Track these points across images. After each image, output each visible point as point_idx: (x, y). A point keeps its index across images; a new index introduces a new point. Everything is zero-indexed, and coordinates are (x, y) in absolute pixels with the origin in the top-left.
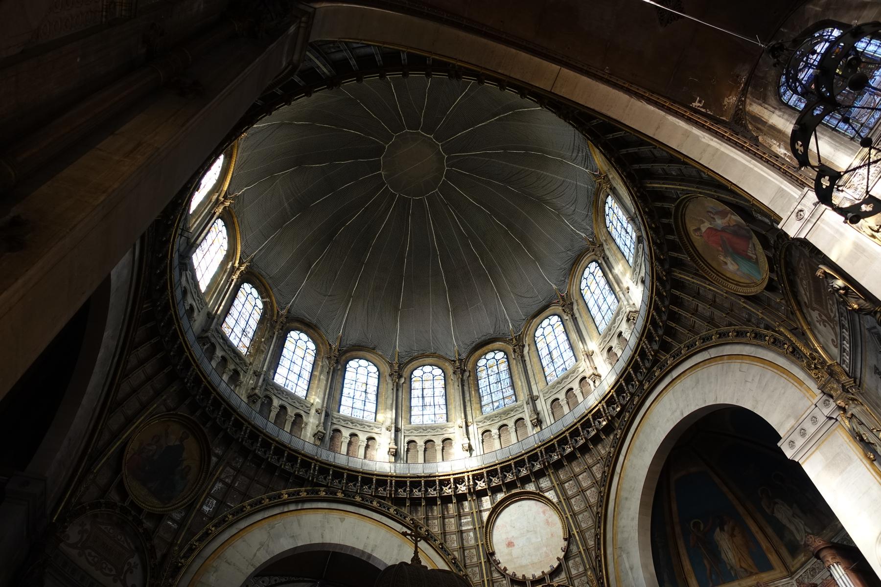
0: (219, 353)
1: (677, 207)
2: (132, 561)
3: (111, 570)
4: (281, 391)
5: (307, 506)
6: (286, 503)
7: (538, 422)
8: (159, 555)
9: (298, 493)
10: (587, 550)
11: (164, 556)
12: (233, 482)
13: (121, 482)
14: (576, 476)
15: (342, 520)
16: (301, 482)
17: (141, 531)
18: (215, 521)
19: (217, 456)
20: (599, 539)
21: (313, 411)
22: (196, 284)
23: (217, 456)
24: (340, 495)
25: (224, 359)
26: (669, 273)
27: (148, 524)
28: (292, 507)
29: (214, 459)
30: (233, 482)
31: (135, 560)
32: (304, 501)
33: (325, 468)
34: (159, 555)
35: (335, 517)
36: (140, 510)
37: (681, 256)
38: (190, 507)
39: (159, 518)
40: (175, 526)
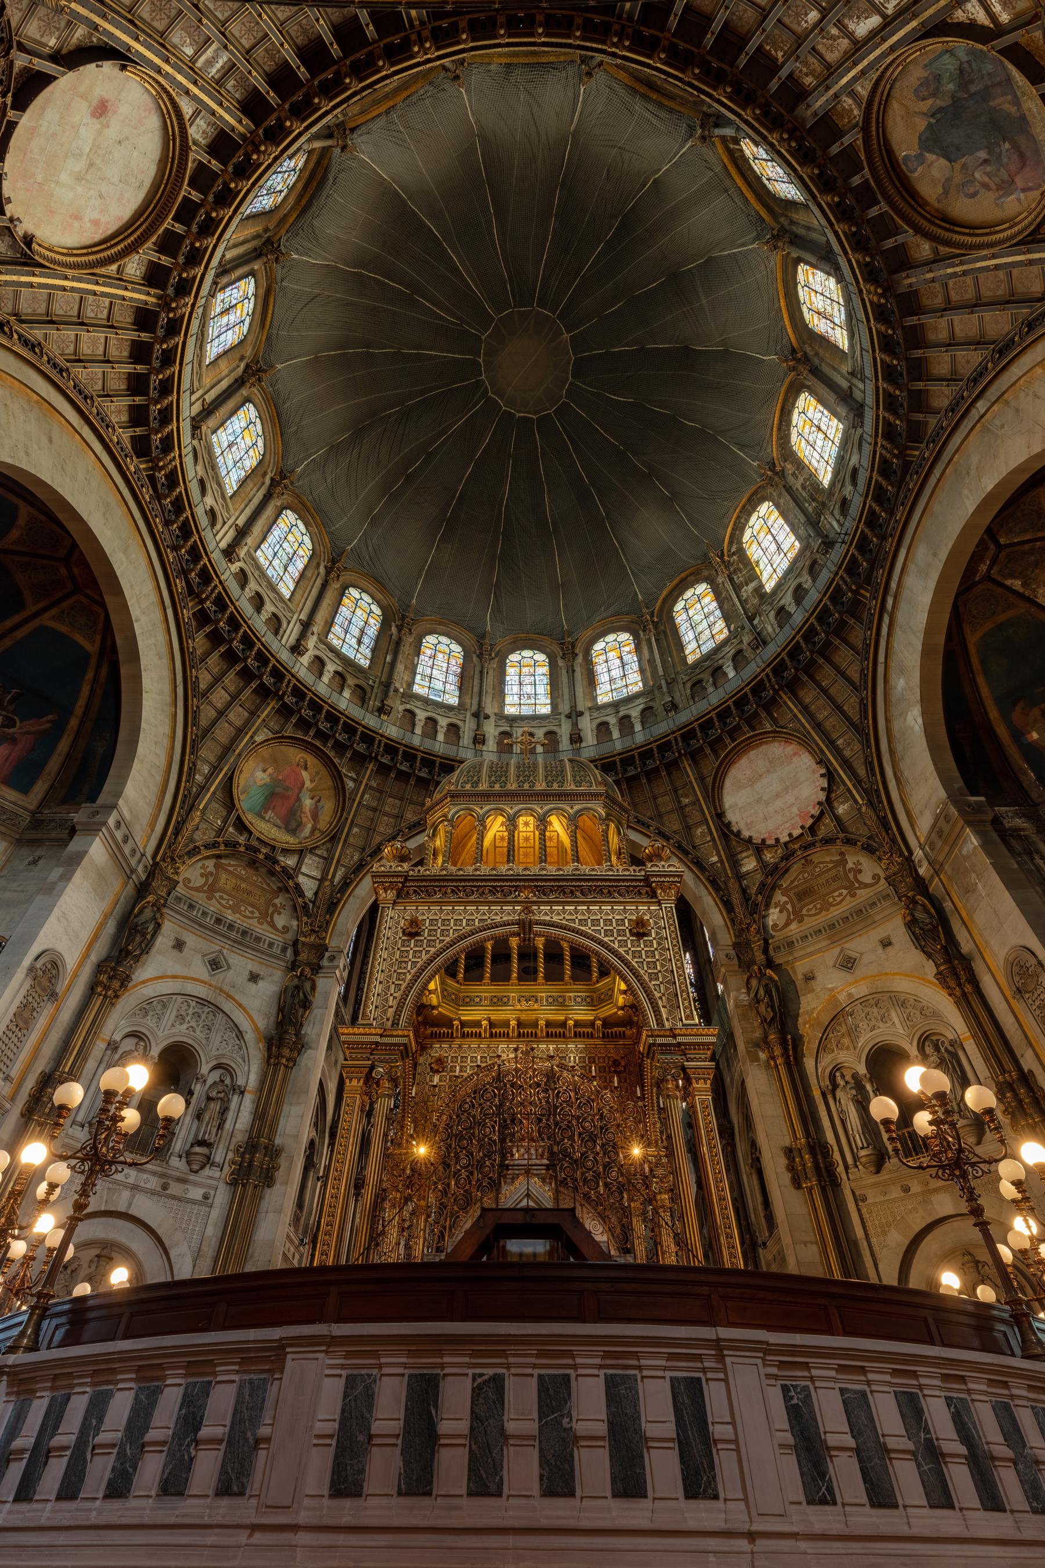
0: (331, 667)
1: (865, 129)
2: (277, 901)
3: (252, 913)
7: (760, 641)
10: (858, 781)
13: (239, 818)
14: (825, 691)
17: (278, 868)
18: (368, 851)
19: (351, 778)
20: (871, 763)
22: (274, 589)
23: (351, 778)
26: (888, 289)
29: (350, 784)
37: (900, 239)
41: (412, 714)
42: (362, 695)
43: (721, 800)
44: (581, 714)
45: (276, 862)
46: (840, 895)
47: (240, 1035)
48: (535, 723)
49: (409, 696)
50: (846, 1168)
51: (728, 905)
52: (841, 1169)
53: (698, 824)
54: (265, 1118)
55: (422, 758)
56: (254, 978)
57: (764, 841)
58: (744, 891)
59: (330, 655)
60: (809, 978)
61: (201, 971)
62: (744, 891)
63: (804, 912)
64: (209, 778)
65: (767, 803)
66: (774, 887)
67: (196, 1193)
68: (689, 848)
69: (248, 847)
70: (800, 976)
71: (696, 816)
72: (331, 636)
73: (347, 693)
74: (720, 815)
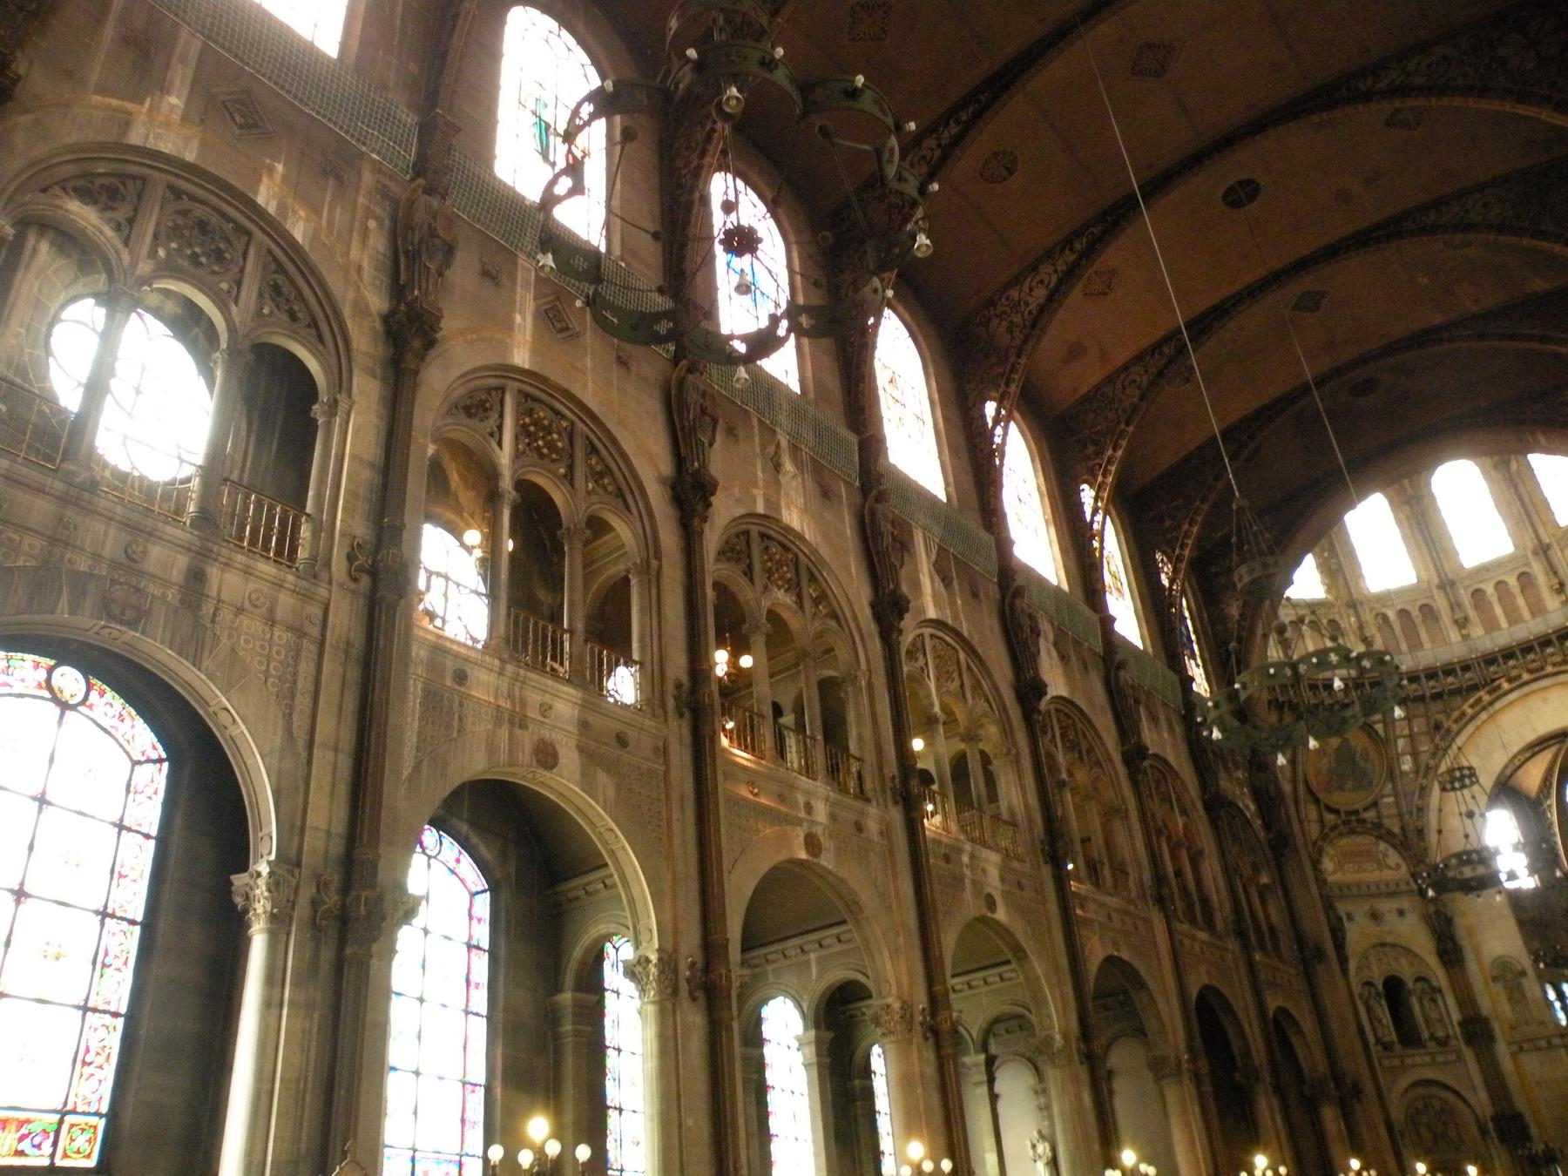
4: (1385, 598)
5: (1498, 705)
6: (1473, 718)
8: (1396, 830)
9: (1480, 700)
11: (1402, 828)
12: (1411, 729)
15: (1545, 700)
16: (1475, 688)
21: (1435, 592)
24: (1526, 676)
27: (1370, 815)
28: (1484, 716)
29: (1379, 727)
30: (1411, 729)
31: (1382, 846)
32: (1491, 703)
33: (1490, 659)
34: (1396, 830)
35: (1535, 702)
36: (1356, 812)
38: (1391, 776)
39: (1375, 804)
40: (1391, 799)
44: (1549, 547)
45: (1364, 821)
47: (1416, 955)
54: (1467, 1000)
56: (1401, 913)
61: (1367, 924)
64: (1295, 788)
69: (1344, 823)
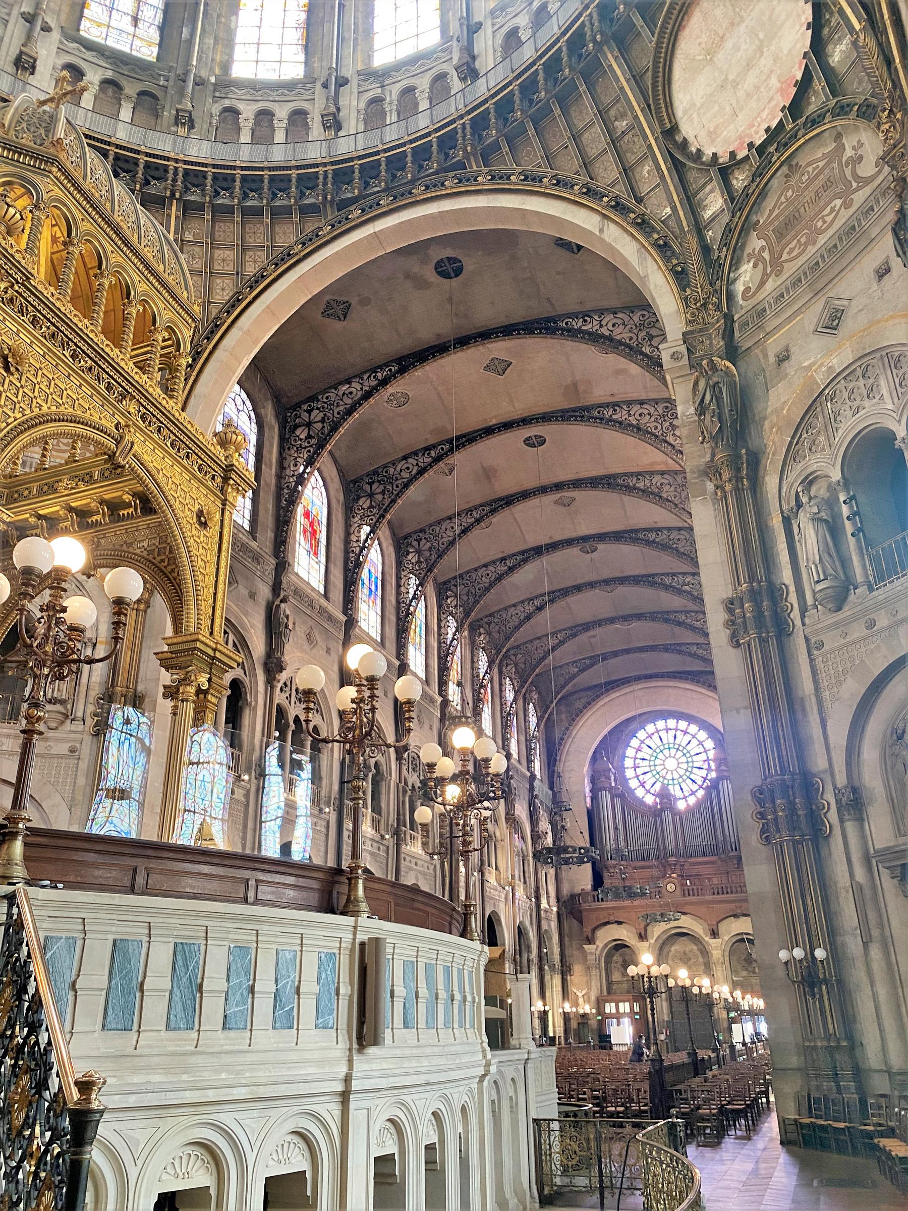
0: (93, 77)
25: (107, 83)
41: (233, 112)
42: (148, 102)
43: (669, 104)
46: (833, 210)
48: (414, 69)
49: (225, 85)
50: (803, 611)
51: (680, 277)
52: (796, 614)
53: (641, 161)
55: (215, 177)
57: (733, 154)
58: (706, 249)
59: (88, 55)
60: (783, 358)
62: (706, 249)
63: (785, 257)
65: (735, 85)
66: (747, 228)
67: (64, 748)
68: (631, 203)
70: (772, 359)
71: (639, 147)
72: (84, 24)
73: (126, 113)
74: (670, 132)
